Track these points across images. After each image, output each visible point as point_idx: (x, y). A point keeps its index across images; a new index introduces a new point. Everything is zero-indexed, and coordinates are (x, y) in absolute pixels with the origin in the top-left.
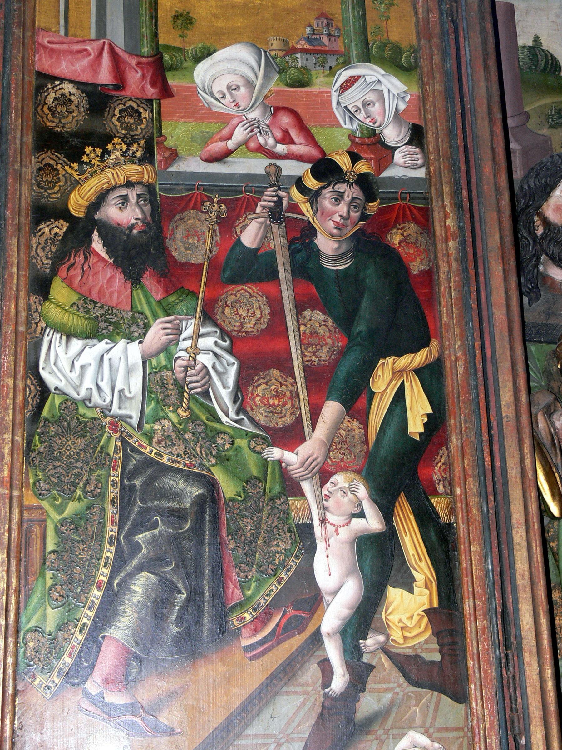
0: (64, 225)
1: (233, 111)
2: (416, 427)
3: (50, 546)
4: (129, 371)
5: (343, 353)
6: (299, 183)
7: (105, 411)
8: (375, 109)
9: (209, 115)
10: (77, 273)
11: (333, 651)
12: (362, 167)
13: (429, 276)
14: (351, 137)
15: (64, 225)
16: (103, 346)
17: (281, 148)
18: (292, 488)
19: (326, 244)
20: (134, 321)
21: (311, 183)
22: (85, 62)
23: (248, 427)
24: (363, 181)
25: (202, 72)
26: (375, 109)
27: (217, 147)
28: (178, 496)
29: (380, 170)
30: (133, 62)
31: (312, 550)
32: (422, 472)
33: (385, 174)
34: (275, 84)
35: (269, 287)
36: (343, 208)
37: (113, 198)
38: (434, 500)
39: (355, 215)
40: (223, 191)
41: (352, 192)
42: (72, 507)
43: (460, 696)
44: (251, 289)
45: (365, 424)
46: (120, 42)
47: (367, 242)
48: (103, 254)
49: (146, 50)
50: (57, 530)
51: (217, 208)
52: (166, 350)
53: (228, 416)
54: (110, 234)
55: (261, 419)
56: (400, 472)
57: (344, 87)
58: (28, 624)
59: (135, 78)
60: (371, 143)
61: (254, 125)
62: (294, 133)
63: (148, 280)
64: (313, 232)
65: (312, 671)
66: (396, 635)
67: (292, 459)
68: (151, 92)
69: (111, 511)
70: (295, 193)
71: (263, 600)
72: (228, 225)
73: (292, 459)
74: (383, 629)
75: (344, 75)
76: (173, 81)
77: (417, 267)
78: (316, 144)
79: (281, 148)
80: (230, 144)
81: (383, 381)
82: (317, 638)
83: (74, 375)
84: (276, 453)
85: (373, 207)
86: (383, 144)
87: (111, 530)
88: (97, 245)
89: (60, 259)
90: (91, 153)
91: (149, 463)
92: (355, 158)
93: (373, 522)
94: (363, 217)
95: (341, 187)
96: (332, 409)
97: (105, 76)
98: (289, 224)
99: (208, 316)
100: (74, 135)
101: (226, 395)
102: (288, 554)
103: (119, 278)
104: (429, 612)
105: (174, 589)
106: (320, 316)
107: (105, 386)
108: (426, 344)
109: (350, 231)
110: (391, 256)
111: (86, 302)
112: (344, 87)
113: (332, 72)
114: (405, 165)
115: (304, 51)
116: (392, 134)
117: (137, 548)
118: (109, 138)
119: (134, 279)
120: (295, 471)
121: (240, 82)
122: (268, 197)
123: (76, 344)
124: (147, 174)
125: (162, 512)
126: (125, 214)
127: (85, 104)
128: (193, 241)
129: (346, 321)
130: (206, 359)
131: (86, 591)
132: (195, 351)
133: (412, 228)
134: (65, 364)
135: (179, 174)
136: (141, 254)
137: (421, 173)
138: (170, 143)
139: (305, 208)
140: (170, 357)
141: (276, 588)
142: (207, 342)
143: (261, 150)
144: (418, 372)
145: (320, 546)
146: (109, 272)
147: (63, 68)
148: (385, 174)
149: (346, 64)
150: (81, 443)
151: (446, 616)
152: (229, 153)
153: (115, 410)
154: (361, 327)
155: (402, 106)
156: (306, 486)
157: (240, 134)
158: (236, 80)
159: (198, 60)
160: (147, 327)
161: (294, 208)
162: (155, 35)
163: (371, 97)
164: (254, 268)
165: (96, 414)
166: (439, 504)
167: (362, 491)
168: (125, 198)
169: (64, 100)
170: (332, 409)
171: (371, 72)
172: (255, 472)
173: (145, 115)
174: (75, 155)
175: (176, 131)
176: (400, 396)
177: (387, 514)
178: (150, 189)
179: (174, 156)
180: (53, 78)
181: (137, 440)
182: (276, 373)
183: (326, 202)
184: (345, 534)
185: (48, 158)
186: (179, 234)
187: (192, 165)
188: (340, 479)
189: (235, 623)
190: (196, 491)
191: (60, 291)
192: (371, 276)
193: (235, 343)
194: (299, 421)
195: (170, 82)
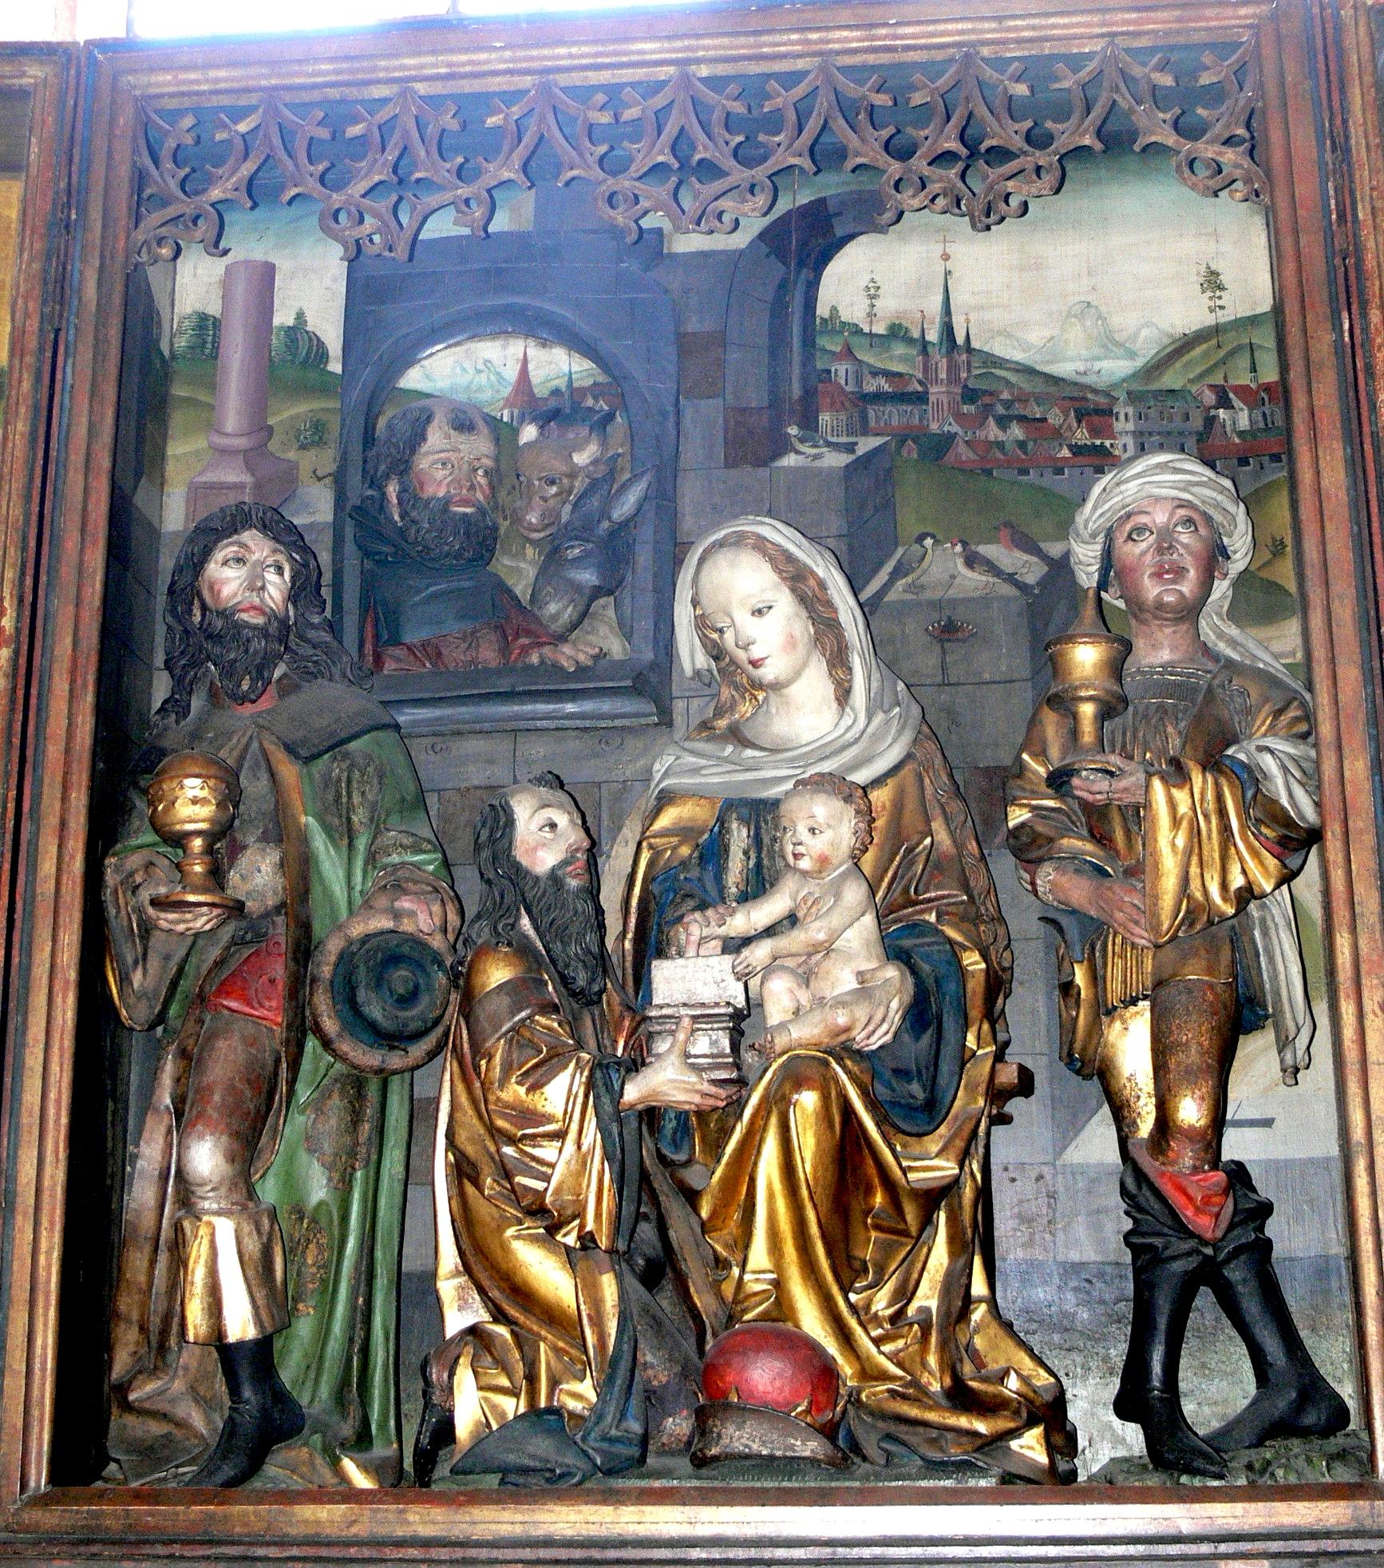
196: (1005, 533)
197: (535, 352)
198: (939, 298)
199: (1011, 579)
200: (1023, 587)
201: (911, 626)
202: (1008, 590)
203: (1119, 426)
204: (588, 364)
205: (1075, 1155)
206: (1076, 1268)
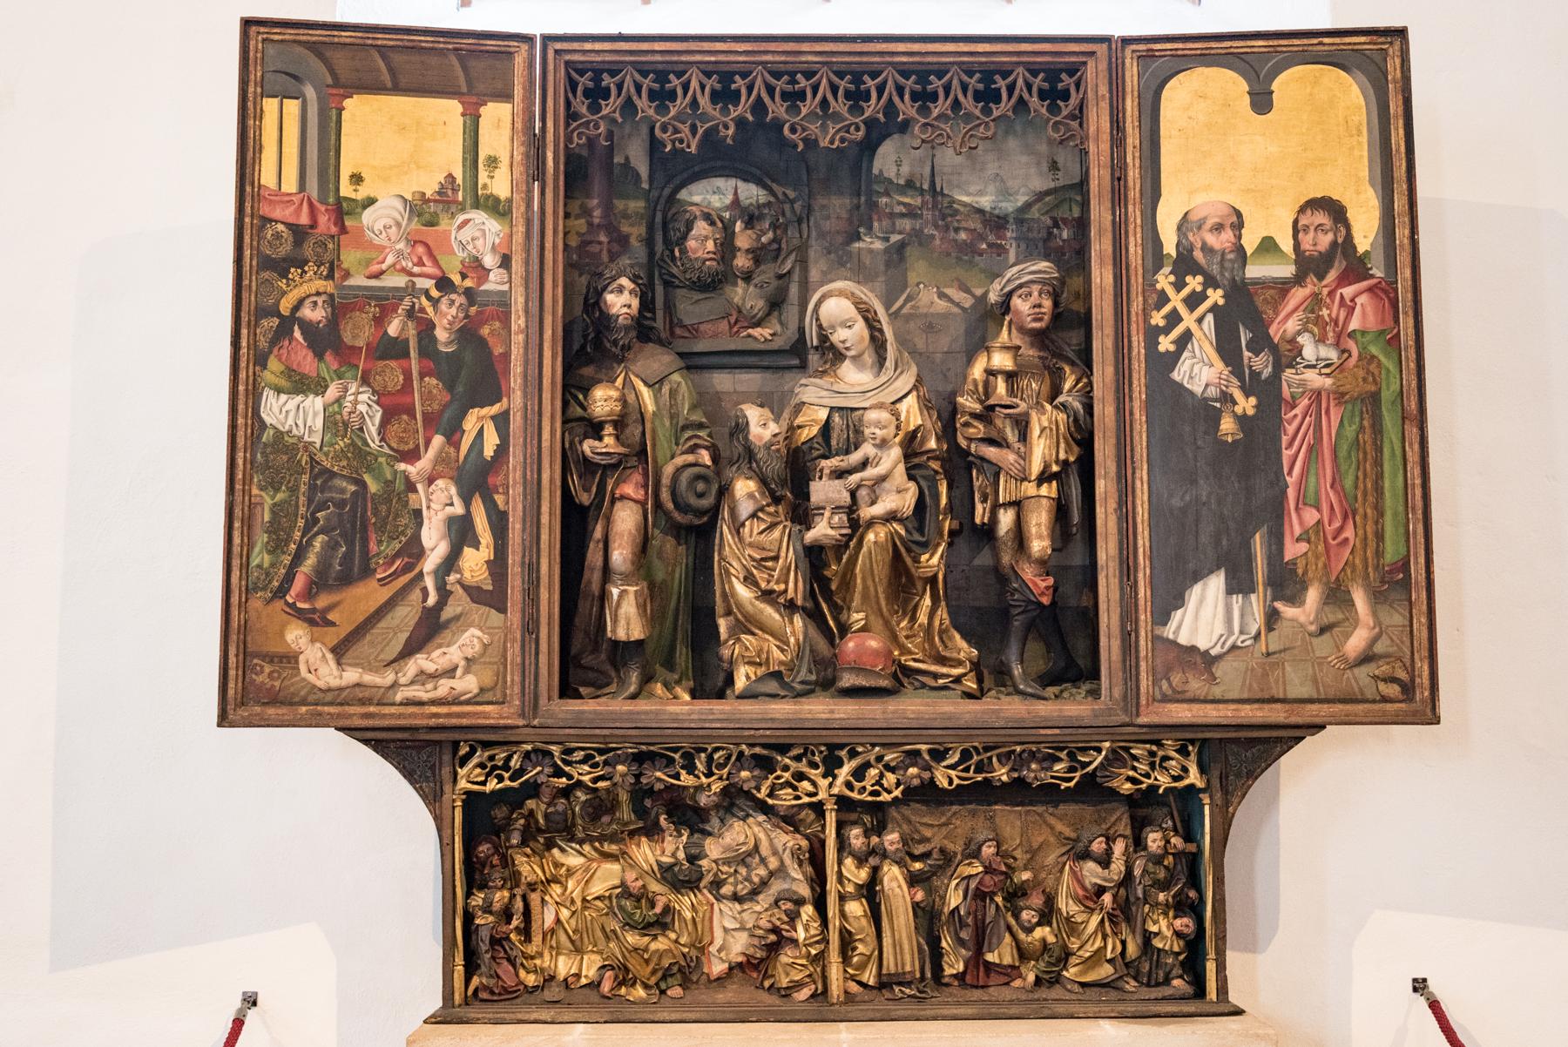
0: (276, 321)
1: (385, 243)
2: (489, 452)
3: (267, 518)
4: (315, 414)
5: (446, 406)
6: (427, 293)
7: (300, 438)
8: (479, 243)
9: (372, 246)
10: (284, 351)
11: (429, 582)
12: (468, 283)
13: (506, 356)
14: (462, 262)
15: (276, 321)
16: (299, 398)
17: (416, 270)
18: (411, 487)
19: (441, 335)
20: (318, 383)
21: (435, 293)
22: (292, 208)
23: (386, 450)
24: (469, 293)
25: (368, 216)
26: (479, 243)
27: (375, 268)
28: (343, 491)
29: (480, 284)
30: (323, 208)
31: (420, 524)
32: (490, 480)
33: (484, 287)
34: (415, 225)
35: (403, 362)
36: (453, 311)
37: (308, 301)
38: (496, 497)
39: (461, 315)
40: (377, 298)
41: (460, 300)
42: (280, 496)
43: (502, 610)
44: (393, 364)
45: (458, 449)
46: (315, 195)
47: (467, 334)
48: (301, 339)
49: (331, 200)
50: (273, 512)
51: (373, 310)
52: (338, 401)
53: (374, 443)
54: (307, 327)
55: (395, 445)
56: (477, 479)
57: (460, 227)
58: (255, 562)
59: (323, 219)
60: (475, 266)
61: (400, 253)
62: (425, 259)
63: (328, 357)
64: (433, 326)
65: (416, 594)
66: (467, 575)
67: (412, 470)
68: (334, 230)
69: (302, 499)
70: (423, 299)
71: (390, 552)
72: (380, 321)
73: (412, 470)
74: (459, 571)
75: (461, 218)
76: (348, 223)
77: (498, 350)
78: (439, 267)
79: (416, 270)
80: (384, 266)
81: (471, 423)
82: (421, 574)
83: (282, 417)
84: (402, 466)
85: (473, 310)
86: (483, 268)
87: (302, 510)
88: (297, 334)
89: (274, 341)
90: (294, 273)
91: (326, 471)
92: (464, 276)
93: (458, 509)
94: (467, 316)
95: (453, 296)
96: (438, 440)
97: (304, 219)
98: (420, 321)
99: (365, 381)
100: (284, 260)
101: (374, 430)
102: (406, 526)
103: (310, 355)
104: (487, 562)
105: (338, 544)
106: (434, 381)
107: (300, 423)
108: (499, 400)
109: (457, 326)
110: (482, 342)
111: (289, 372)
112: (460, 227)
113: (453, 216)
114: (495, 282)
115: (435, 201)
116: (489, 261)
117: (316, 521)
118: (306, 262)
119: (319, 356)
120: (413, 478)
121: (392, 223)
122: (407, 303)
123: (283, 397)
124: (329, 287)
125: (331, 500)
126: (315, 314)
127: (291, 238)
128: (358, 332)
129: (450, 387)
130: (362, 408)
131: (287, 545)
132: (356, 403)
133: (498, 324)
134: (276, 410)
135: (351, 287)
136: (324, 340)
137: (506, 287)
138: (345, 265)
139: (430, 310)
140: (340, 406)
141: (398, 546)
142: (363, 397)
143: (404, 271)
144: (493, 418)
145: (426, 521)
146: (305, 351)
147: (277, 213)
148: (484, 287)
149: (463, 210)
150: (285, 458)
151: (497, 566)
152: (382, 273)
153: (306, 438)
154: (460, 389)
155: (497, 241)
156: (420, 487)
157: (390, 260)
158: (390, 222)
159: (365, 207)
160: (326, 387)
161: (422, 310)
162: (338, 189)
163: (478, 234)
164: (393, 349)
165: (294, 440)
166: (499, 499)
167: (453, 490)
168: (315, 303)
169: (278, 236)
170: (438, 440)
171: (479, 216)
172: (389, 477)
173: (331, 246)
174: (284, 274)
175: (349, 258)
176: (481, 431)
177: (467, 502)
178: (331, 296)
179: (347, 275)
180: (271, 220)
181: (319, 457)
182: (405, 417)
183: (443, 306)
184: (441, 516)
185: (266, 275)
186: (350, 326)
187: (359, 280)
188: (440, 483)
189: (373, 566)
190: (353, 488)
191: (274, 364)
192: (468, 356)
193: (381, 396)
194: (418, 446)
195: (347, 223)
196: (956, 284)
197: (740, 184)
198: (927, 170)
199: (958, 305)
200: (963, 309)
201: (912, 325)
202: (956, 310)
203: (1009, 234)
204: (762, 192)
205: (977, 562)
206: (978, 609)
